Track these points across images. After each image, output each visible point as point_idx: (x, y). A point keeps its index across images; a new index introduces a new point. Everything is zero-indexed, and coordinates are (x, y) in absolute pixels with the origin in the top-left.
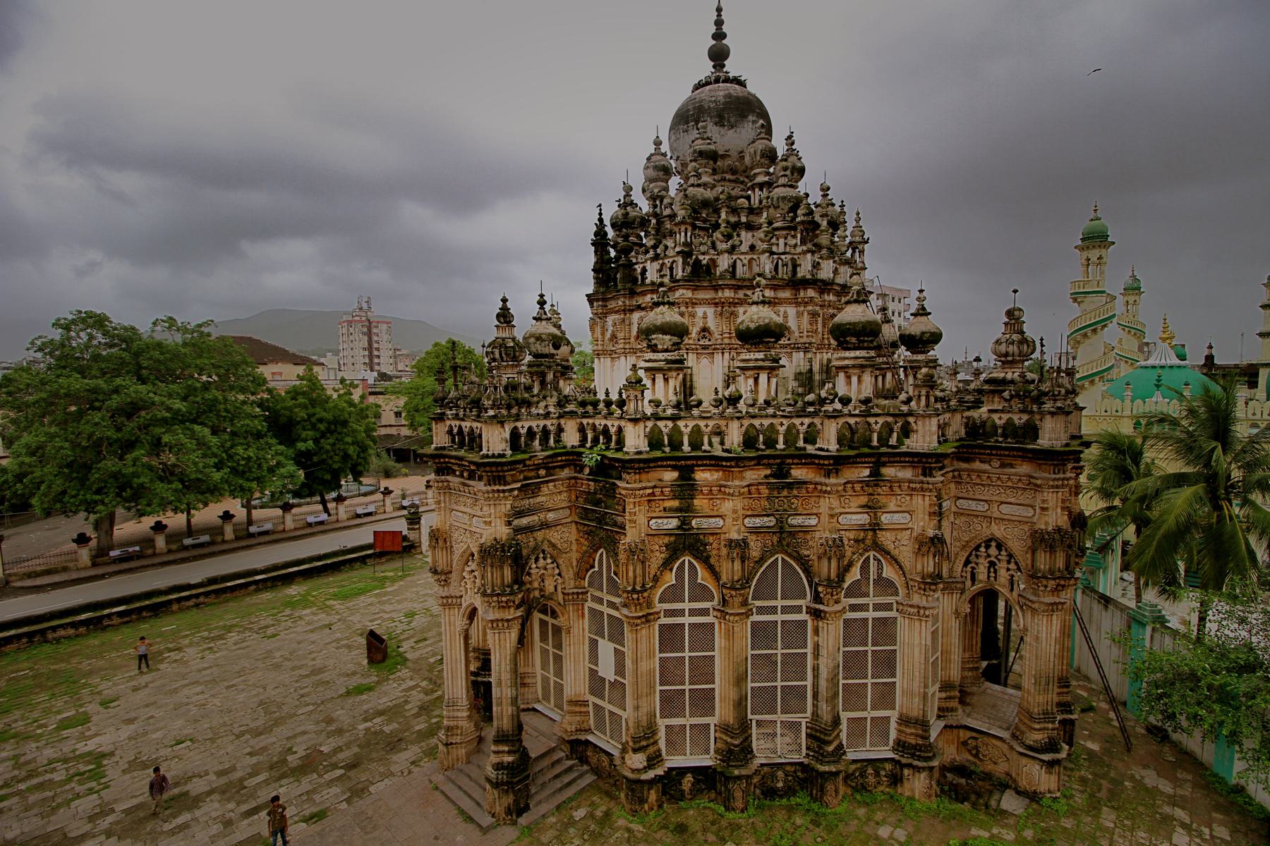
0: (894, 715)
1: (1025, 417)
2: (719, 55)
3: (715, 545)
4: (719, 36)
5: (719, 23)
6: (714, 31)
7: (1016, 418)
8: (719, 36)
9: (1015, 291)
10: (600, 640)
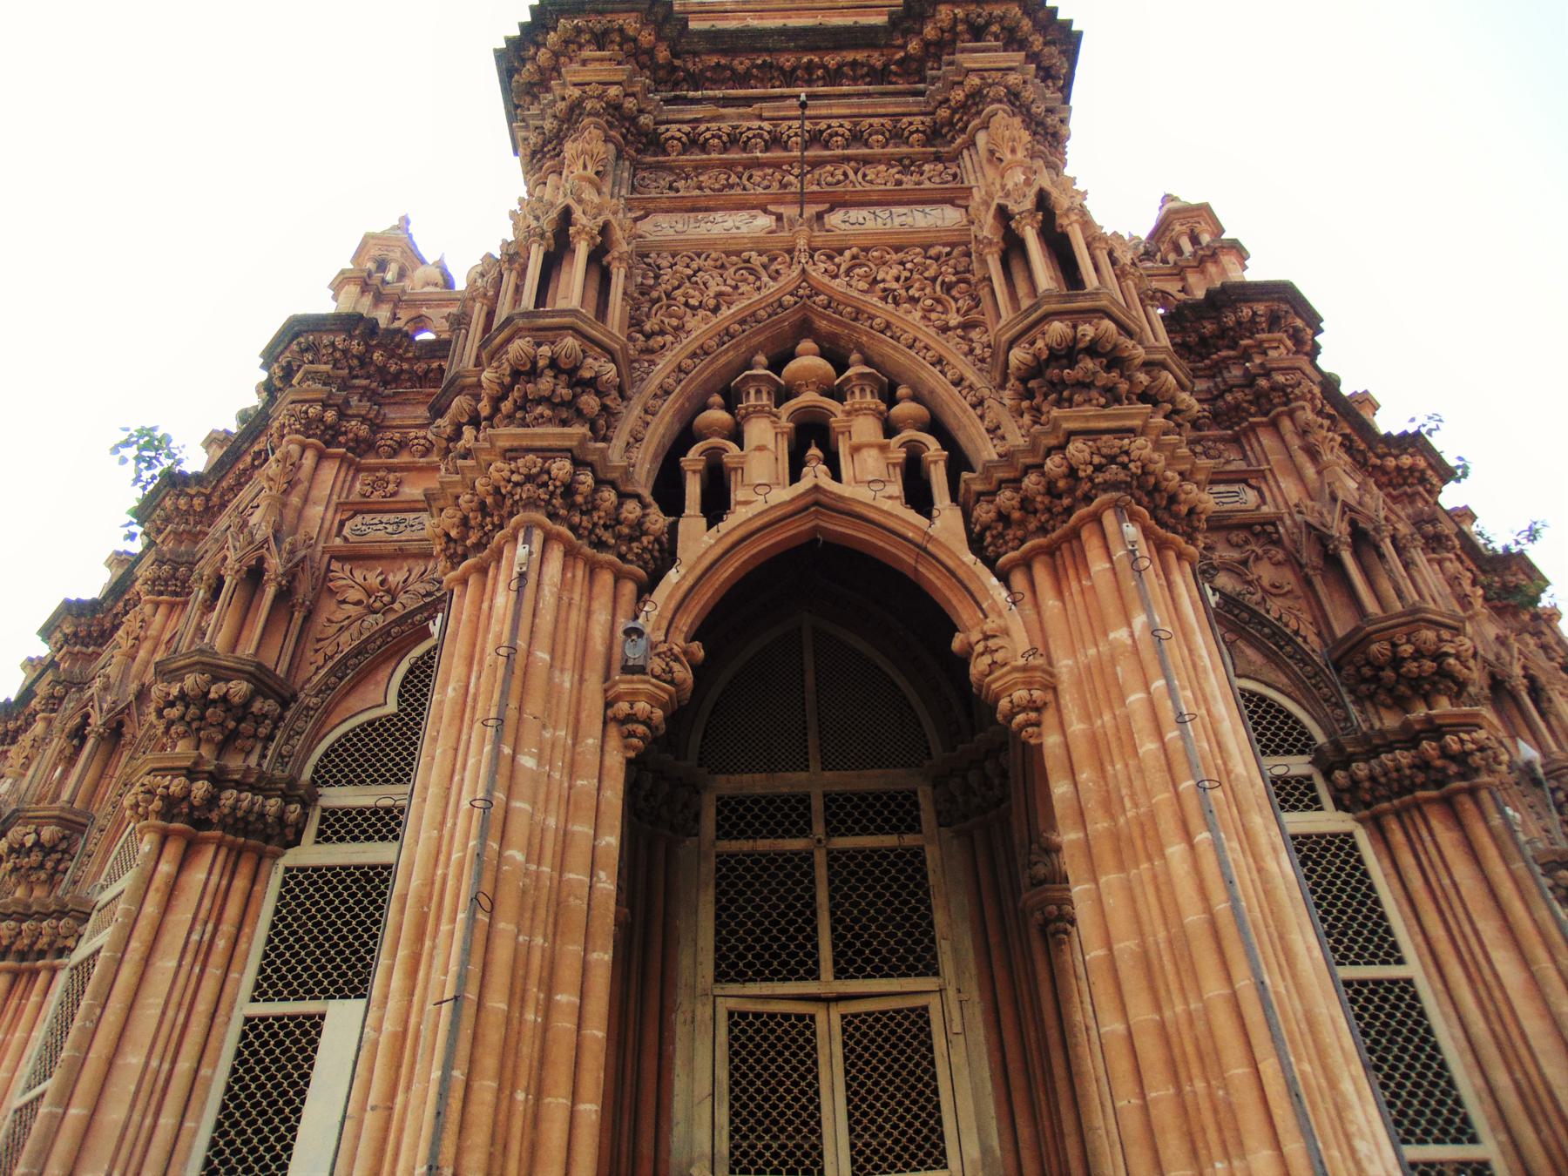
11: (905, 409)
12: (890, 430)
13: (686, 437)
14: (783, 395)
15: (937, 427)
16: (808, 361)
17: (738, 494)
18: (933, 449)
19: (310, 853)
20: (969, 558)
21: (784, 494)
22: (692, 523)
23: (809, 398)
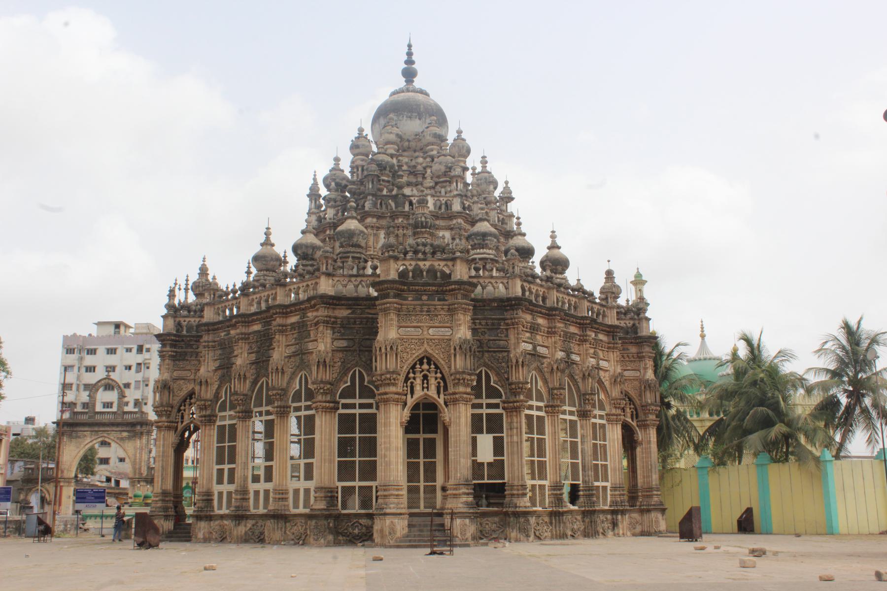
0: (608, 484)
1: (632, 322)
2: (409, 74)
4: (410, 62)
5: (410, 54)
6: (406, 58)
10: (479, 437)
12: (436, 378)
13: (407, 379)
14: (421, 372)
15: (443, 378)
16: (425, 366)
17: (416, 392)
18: (442, 384)
19: (341, 411)
20: (444, 406)
21: (422, 393)
22: (409, 396)
23: (425, 372)
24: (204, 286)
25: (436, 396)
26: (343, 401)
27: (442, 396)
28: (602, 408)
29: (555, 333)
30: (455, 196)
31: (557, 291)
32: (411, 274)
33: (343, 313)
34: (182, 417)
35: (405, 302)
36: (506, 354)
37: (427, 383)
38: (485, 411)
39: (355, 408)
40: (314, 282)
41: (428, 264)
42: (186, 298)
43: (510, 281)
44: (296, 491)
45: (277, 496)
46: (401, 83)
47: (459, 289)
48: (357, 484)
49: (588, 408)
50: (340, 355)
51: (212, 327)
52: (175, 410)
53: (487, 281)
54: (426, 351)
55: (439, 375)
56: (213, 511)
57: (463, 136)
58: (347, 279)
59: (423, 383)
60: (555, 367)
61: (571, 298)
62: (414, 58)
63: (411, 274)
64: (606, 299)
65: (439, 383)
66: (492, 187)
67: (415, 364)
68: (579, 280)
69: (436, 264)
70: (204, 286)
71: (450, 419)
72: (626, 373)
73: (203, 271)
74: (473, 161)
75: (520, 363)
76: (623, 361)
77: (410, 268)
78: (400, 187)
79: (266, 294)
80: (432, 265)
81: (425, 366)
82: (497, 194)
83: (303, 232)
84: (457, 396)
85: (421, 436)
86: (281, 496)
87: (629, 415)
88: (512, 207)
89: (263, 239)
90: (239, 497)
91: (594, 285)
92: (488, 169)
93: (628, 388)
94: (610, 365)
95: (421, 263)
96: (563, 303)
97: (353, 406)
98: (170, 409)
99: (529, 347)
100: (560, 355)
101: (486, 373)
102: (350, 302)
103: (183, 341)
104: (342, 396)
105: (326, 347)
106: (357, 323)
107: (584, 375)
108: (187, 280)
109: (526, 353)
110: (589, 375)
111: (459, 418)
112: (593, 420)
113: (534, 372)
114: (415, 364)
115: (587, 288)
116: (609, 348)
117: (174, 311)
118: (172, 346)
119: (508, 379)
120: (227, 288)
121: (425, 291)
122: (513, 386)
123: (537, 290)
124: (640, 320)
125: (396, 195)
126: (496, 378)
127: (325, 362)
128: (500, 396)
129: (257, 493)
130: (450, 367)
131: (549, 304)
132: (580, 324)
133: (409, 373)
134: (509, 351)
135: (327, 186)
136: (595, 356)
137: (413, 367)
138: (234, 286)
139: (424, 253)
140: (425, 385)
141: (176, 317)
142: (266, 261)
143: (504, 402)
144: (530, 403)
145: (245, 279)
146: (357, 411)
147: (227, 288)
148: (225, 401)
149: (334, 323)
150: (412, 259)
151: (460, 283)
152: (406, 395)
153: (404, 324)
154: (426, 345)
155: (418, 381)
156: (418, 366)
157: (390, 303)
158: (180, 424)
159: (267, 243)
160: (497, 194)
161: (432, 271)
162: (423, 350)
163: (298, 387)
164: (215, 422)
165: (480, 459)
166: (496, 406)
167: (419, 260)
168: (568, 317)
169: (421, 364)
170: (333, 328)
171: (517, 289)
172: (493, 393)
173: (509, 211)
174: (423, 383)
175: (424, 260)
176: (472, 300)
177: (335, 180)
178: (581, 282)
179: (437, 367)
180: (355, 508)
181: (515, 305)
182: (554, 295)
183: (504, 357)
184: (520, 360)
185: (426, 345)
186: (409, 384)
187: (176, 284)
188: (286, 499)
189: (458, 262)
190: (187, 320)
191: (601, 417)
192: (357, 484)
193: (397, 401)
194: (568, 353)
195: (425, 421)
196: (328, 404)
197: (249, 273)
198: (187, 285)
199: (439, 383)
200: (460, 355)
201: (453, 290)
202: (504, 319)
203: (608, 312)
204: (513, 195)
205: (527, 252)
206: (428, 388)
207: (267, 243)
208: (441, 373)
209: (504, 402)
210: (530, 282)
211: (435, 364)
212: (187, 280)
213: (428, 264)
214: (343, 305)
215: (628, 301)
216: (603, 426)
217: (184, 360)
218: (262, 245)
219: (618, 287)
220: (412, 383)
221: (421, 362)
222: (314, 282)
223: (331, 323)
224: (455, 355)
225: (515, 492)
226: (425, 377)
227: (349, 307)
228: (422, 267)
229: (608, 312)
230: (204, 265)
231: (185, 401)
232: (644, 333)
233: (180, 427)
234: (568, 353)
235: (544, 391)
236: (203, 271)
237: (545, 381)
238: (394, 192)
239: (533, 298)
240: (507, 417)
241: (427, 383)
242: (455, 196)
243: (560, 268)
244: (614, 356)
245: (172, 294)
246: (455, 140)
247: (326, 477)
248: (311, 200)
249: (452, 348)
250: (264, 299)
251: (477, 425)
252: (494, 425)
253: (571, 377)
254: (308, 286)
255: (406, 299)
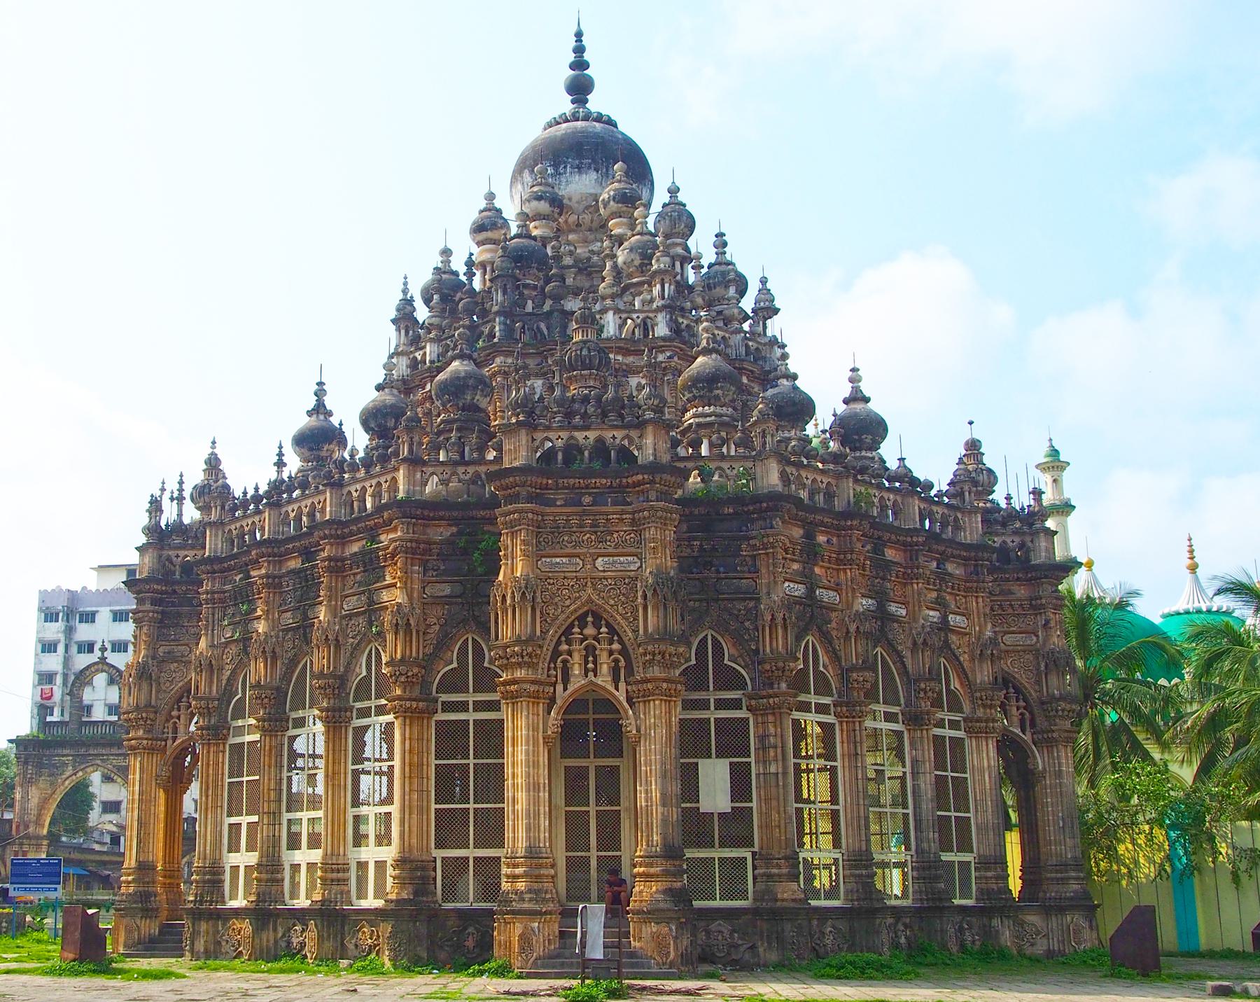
1: (1017, 539)
3: (834, 625)
7: (1009, 540)
8: (580, 64)
9: (971, 423)
10: (701, 762)
11: (616, 646)
12: (611, 653)
13: (556, 653)
14: (582, 641)
15: (624, 652)
16: (590, 631)
18: (622, 663)
20: (625, 704)
22: (560, 687)
24: (213, 491)
25: (611, 688)
26: (444, 697)
27: (622, 685)
28: (955, 706)
29: (851, 562)
30: (659, 310)
31: (856, 481)
32: (560, 456)
33: (441, 533)
34: (175, 730)
35: (548, 510)
36: (752, 604)
37: (595, 663)
38: (713, 715)
39: (467, 710)
40: (389, 477)
41: (592, 435)
42: (180, 515)
43: (758, 464)
44: (362, 866)
45: (330, 875)
46: (565, 105)
47: (652, 482)
48: (471, 853)
49: (925, 705)
50: (439, 611)
51: (217, 565)
52: (160, 719)
53: (713, 465)
54: (590, 601)
55: (616, 646)
56: (224, 902)
57: (681, 197)
58: (448, 470)
59: (586, 662)
60: (853, 628)
61: (886, 495)
62: (587, 56)
63: (560, 456)
64: (960, 495)
65: (616, 661)
66: (732, 291)
67: (572, 626)
68: (902, 460)
69: (608, 435)
70: (213, 491)
71: (638, 731)
72: (1009, 639)
73: (213, 464)
74: (701, 244)
75: (779, 620)
76: (998, 613)
77: (560, 443)
78: (557, 298)
79: (309, 502)
80: (600, 440)
81: (590, 631)
82: (748, 304)
83: (379, 388)
84: (650, 686)
85: (592, 763)
86: (335, 875)
87: (1016, 720)
88: (774, 327)
89: (311, 402)
90: (264, 876)
91: (937, 469)
92: (728, 257)
93: (1008, 665)
94: (969, 620)
95: (579, 435)
96: (883, 508)
97: (463, 707)
98: (152, 716)
99: (799, 590)
100: (864, 604)
101: (716, 644)
102: (455, 514)
103: (175, 592)
104: (445, 687)
105: (410, 598)
106: (457, 547)
107: (915, 643)
108: (181, 483)
109: (790, 603)
110: (925, 643)
111: (653, 730)
112: (938, 731)
113: (810, 638)
114: (572, 626)
115: (920, 474)
116: (967, 590)
117: (160, 537)
118: (154, 602)
119: (757, 651)
120: (245, 493)
121: (587, 487)
122: (767, 667)
123: (814, 480)
124: (1035, 534)
125: (550, 313)
126: (733, 651)
127: (408, 624)
128: (743, 686)
129: (235, 869)
130: (636, 631)
131: (839, 505)
132: (904, 544)
133: (559, 643)
134: (758, 600)
135: (427, 301)
136: (940, 604)
137: (568, 631)
138: (257, 489)
139: (585, 416)
140: (590, 665)
141: (162, 549)
142: (319, 439)
143: (750, 698)
144: (802, 698)
145: (274, 476)
146: (471, 716)
147: (245, 493)
148: (243, 699)
149: (425, 552)
150: (561, 428)
151: (654, 468)
152: (554, 685)
153: (548, 551)
154: (590, 591)
155: (577, 658)
156: (576, 630)
157: (520, 511)
158: (170, 742)
159: (320, 409)
160: (748, 304)
161: (601, 448)
162: (584, 598)
163: (364, 673)
164: (225, 738)
165: (705, 805)
166: (736, 704)
167: (576, 428)
168: (879, 533)
169: (583, 626)
170: (424, 564)
171: (771, 477)
172: (728, 679)
173: (769, 333)
174: (586, 662)
175: (587, 428)
176: (678, 502)
177: (445, 289)
178: (907, 463)
179: (612, 631)
180: (470, 898)
181: (768, 509)
182: (849, 490)
183: (748, 610)
184: (779, 616)
185: (590, 591)
186: (559, 664)
187: (163, 490)
188: (345, 881)
189: (650, 429)
190: (182, 553)
191: (954, 725)
192: (471, 853)
193: (535, 696)
194: (881, 598)
195: (589, 736)
196: (414, 704)
197: (280, 464)
198: (181, 490)
199: (616, 661)
200: (656, 608)
201: (639, 484)
202: (749, 539)
203: (964, 520)
204: (777, 304)
205: (801, 408)
206: (595, 671)
207: (320, 409)
208: (621, 641)
209: (750, 698)
210: (799, 465)
211: (608, 625)
212: (181, 483)
213: (592, 435)
214: (441, 518)
215: (1008, 498)
216: (957, 743)
217: (177, 625)
218: (310, 413)
219: (990, 471)
220: (565, 662)
221: (582, 620)
222: (389, 477)
223: (416, 552)
224: (645, 608)
225: (775, 871)
226: (590, 651)
227: (453, 521)
228: (581, 441)
229: (964, 520)
230: (212, 454)
231: (179, 700)
232: (1039, 558)
233: (172, 747)
234: (881, 598)
235: (830, 674)
236: (213, 464)
237: (835, 657)
238: (546, 308)
239: (803, 494)
240: (756, 726)
241: (595, 663)
242: (659, 310)
243: (868, 439)
244: (978, 604)
245: (155, 506)
246: (665, 206)
247: (414, 841)
248: (398, 330)
249: (640, 594)
250: (305, 511)
251: (691, 742)
252: (732, 741)
253: (891, 647)
254: (379, 484)
255: (552, 503)
